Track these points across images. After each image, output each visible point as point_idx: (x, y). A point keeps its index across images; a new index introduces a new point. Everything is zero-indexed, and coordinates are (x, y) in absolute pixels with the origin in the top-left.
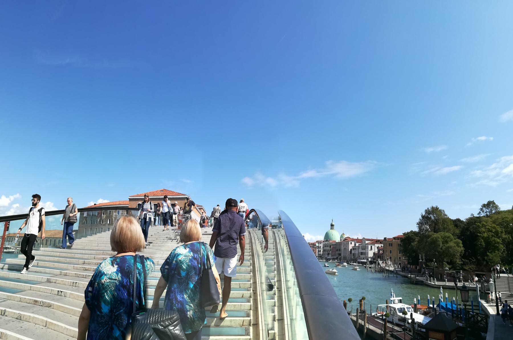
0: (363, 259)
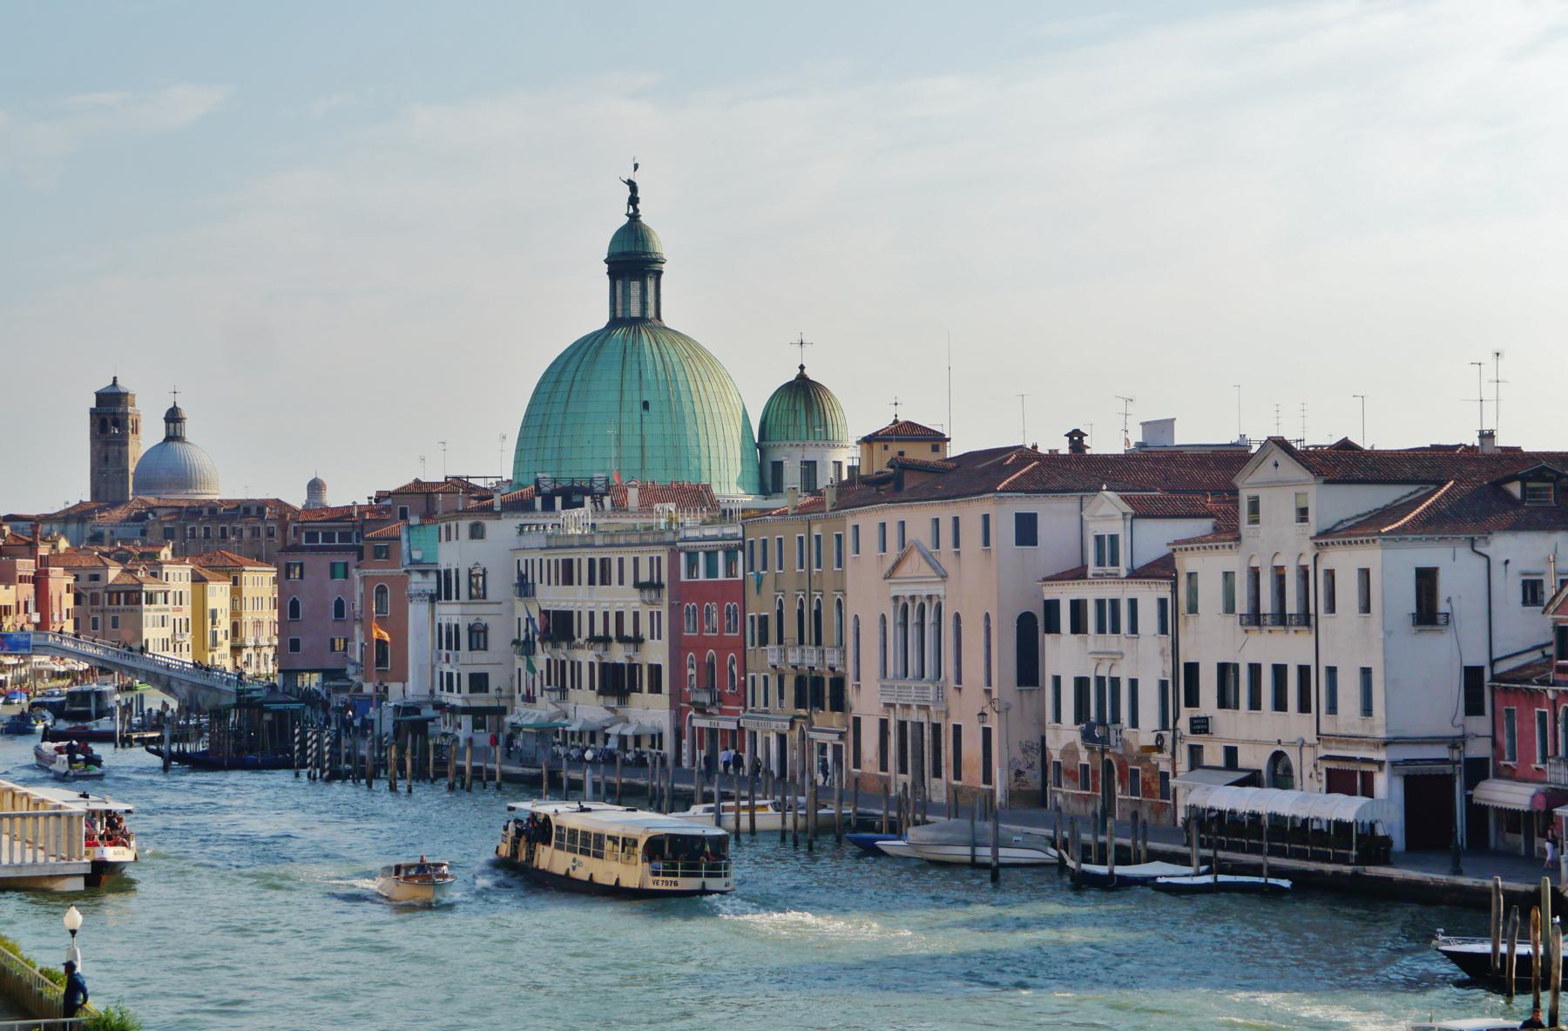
0: (1279, 773)
